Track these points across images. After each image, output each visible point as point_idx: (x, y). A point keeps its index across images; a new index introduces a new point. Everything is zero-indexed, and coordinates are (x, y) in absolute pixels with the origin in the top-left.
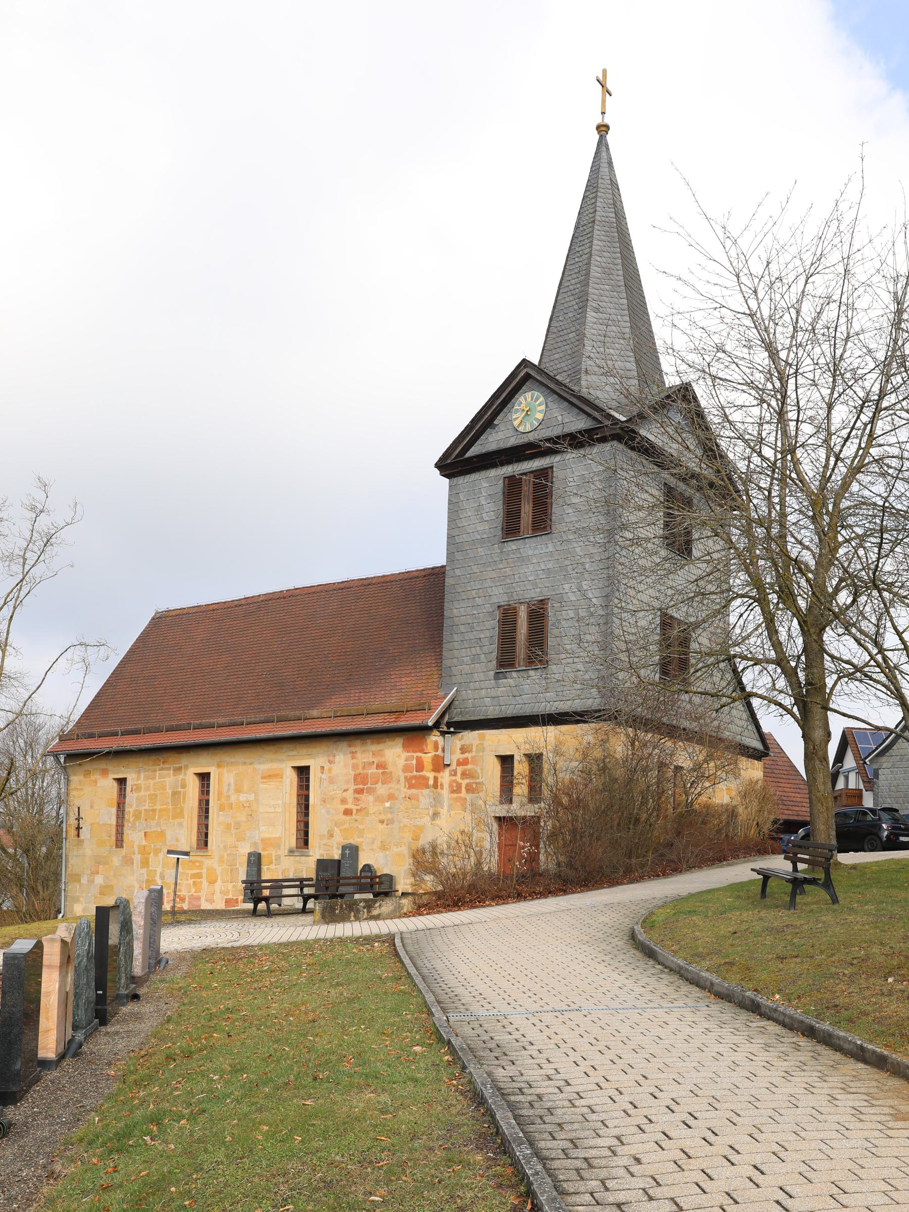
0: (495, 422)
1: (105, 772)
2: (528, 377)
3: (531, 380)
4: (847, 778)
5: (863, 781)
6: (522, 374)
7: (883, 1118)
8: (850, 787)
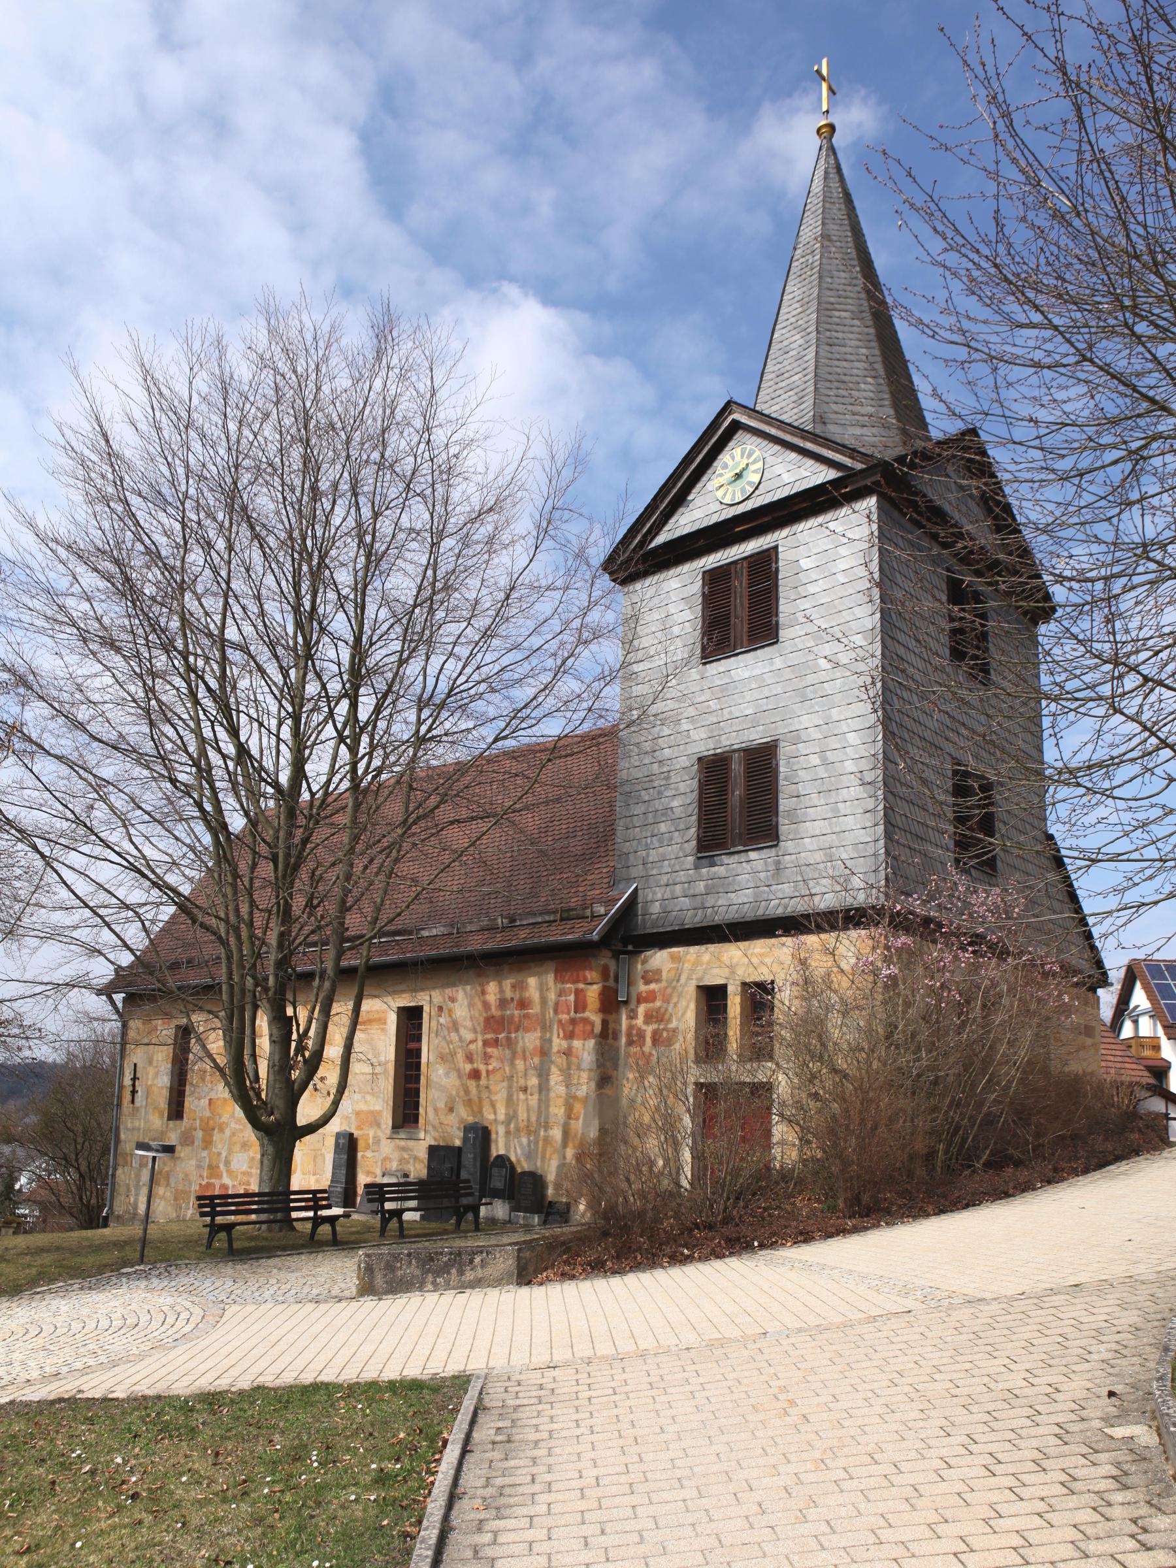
0: (690, 498)
1: (168, 1016)
2: (736, 426)
3: (740, 435)
4: (1136, 1022)
5: (1164, 1027)
6: (726, 424)
7: (1109, 1310)
8: (1141, 1034)
